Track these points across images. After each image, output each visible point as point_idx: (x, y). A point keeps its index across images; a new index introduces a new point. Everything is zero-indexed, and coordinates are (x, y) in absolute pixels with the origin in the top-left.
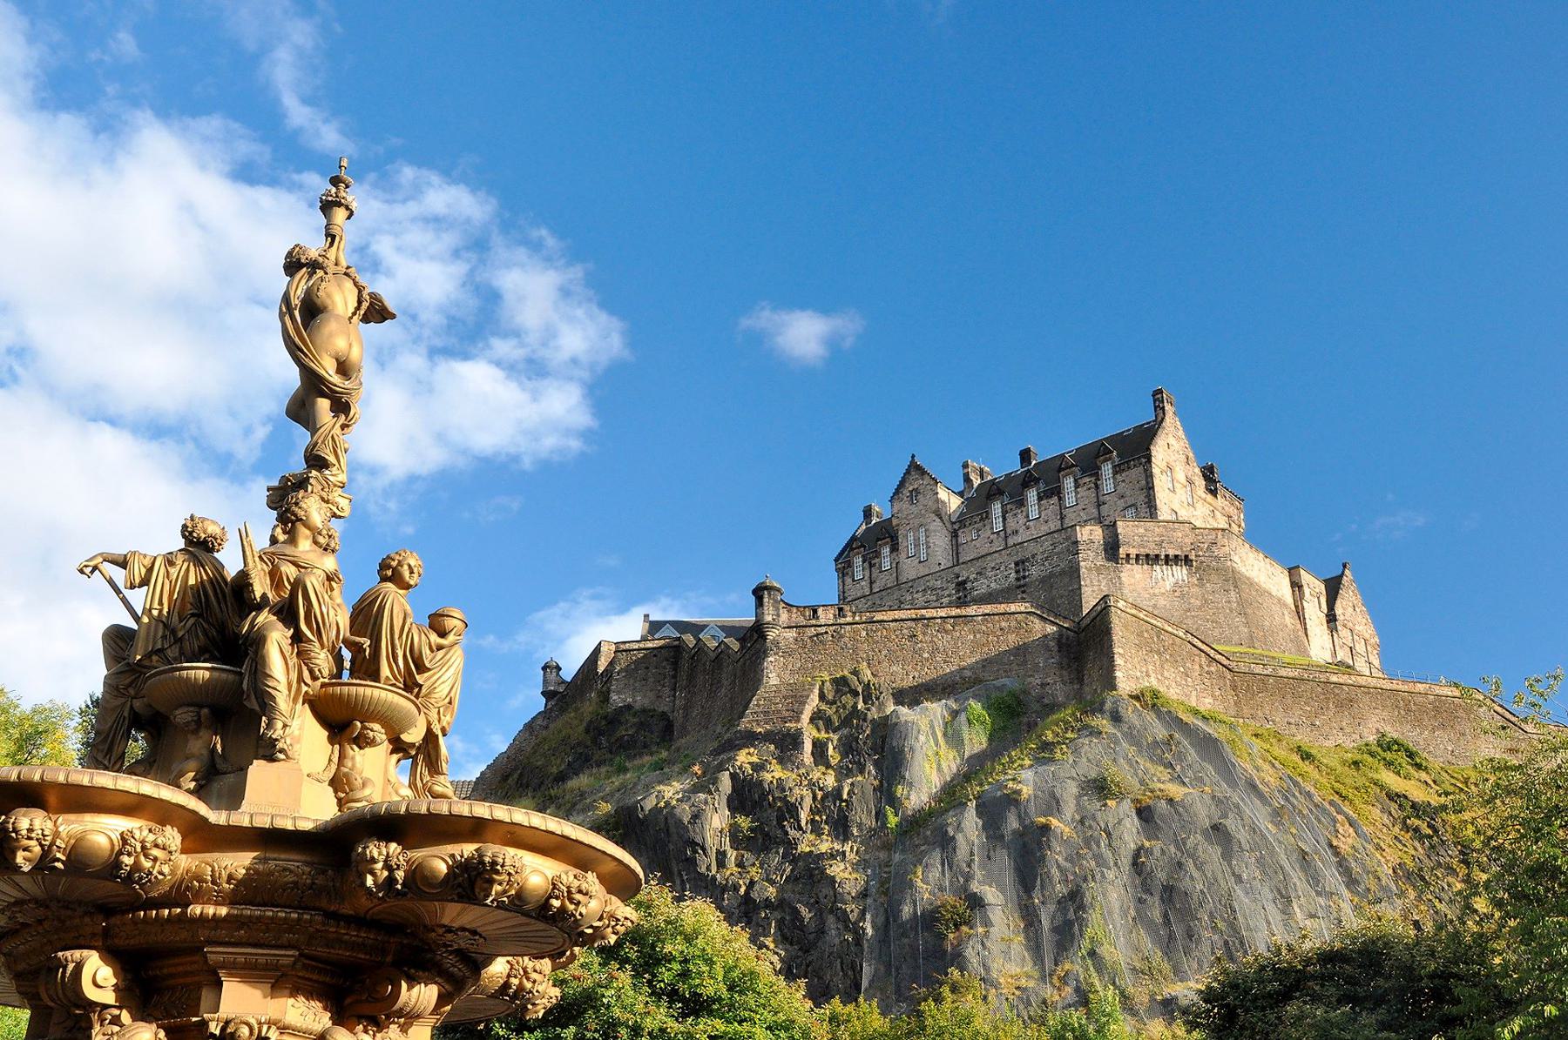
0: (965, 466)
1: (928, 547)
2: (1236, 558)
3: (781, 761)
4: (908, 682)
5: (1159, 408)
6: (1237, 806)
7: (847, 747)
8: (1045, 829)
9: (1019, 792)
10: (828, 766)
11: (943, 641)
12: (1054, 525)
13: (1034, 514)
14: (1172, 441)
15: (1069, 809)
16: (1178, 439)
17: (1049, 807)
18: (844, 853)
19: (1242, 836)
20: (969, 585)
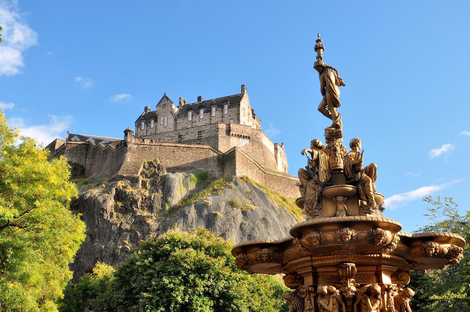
0: (180, 99)
1: (167, 123)
3: (132, 186)
4: (171, 166)
5: (243, 90)
6: (270, 213)
7: (153, 184)
8: (215, 215)
9: (208, 203)
10: (146, 189)
11: (183, 154)
12: (208, 121)
13: (202, 117)
15: (223, 210)
16: (247, 101)
17: (217, 208)
18: (152, 217)
19: (271, 222)
20: (182, 137)
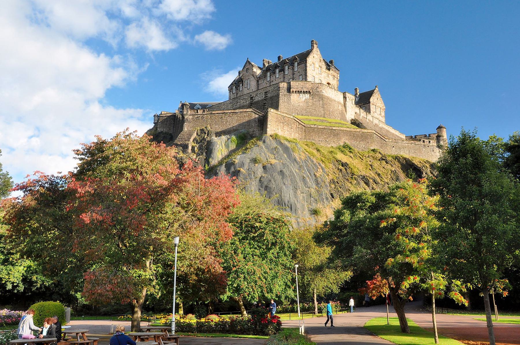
0: (264, 61)
2: (324, 91)
3: (183, 152)
4: (220, 130)
5: (312, 46)
6: (288, 166)
7: (200, 148)
8: (239, 171)
9: (234, 162)
10: (195, 153)
11: (229, 119)
13: (277, 76)
14: (315, 55)
15: (246, 167)
16: (317, 55)
17: (241, 165)
19: (287, 172)
